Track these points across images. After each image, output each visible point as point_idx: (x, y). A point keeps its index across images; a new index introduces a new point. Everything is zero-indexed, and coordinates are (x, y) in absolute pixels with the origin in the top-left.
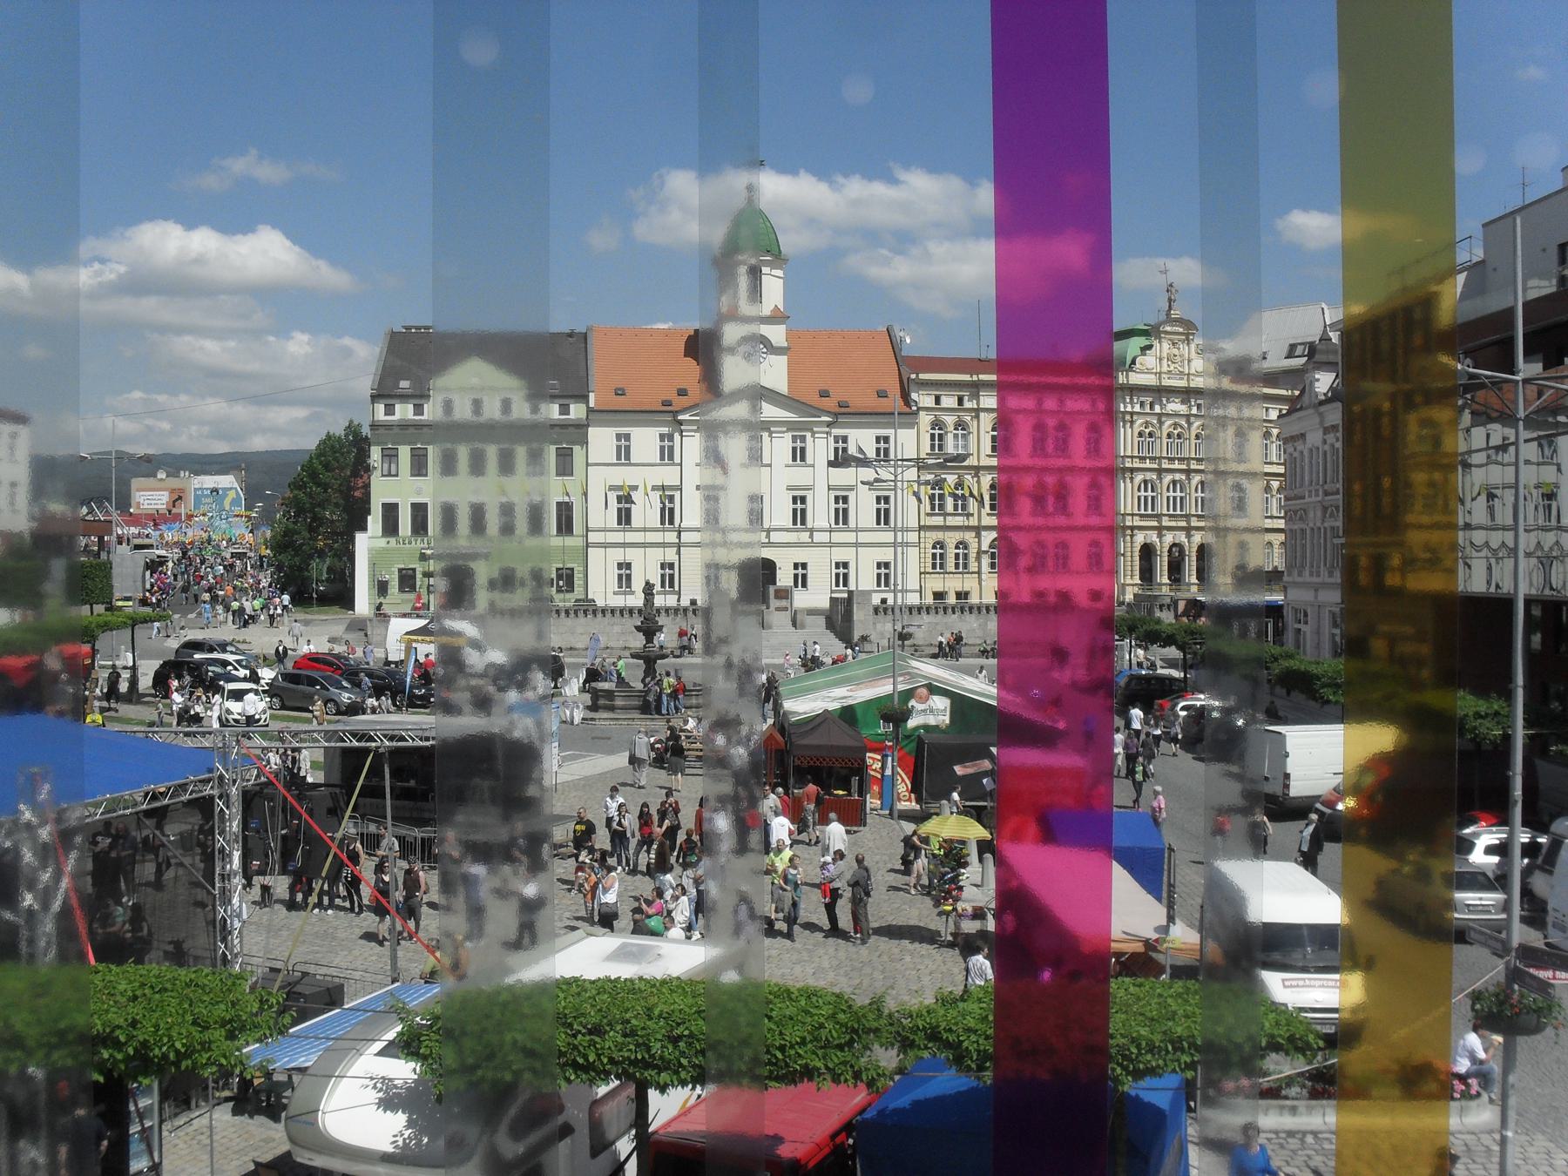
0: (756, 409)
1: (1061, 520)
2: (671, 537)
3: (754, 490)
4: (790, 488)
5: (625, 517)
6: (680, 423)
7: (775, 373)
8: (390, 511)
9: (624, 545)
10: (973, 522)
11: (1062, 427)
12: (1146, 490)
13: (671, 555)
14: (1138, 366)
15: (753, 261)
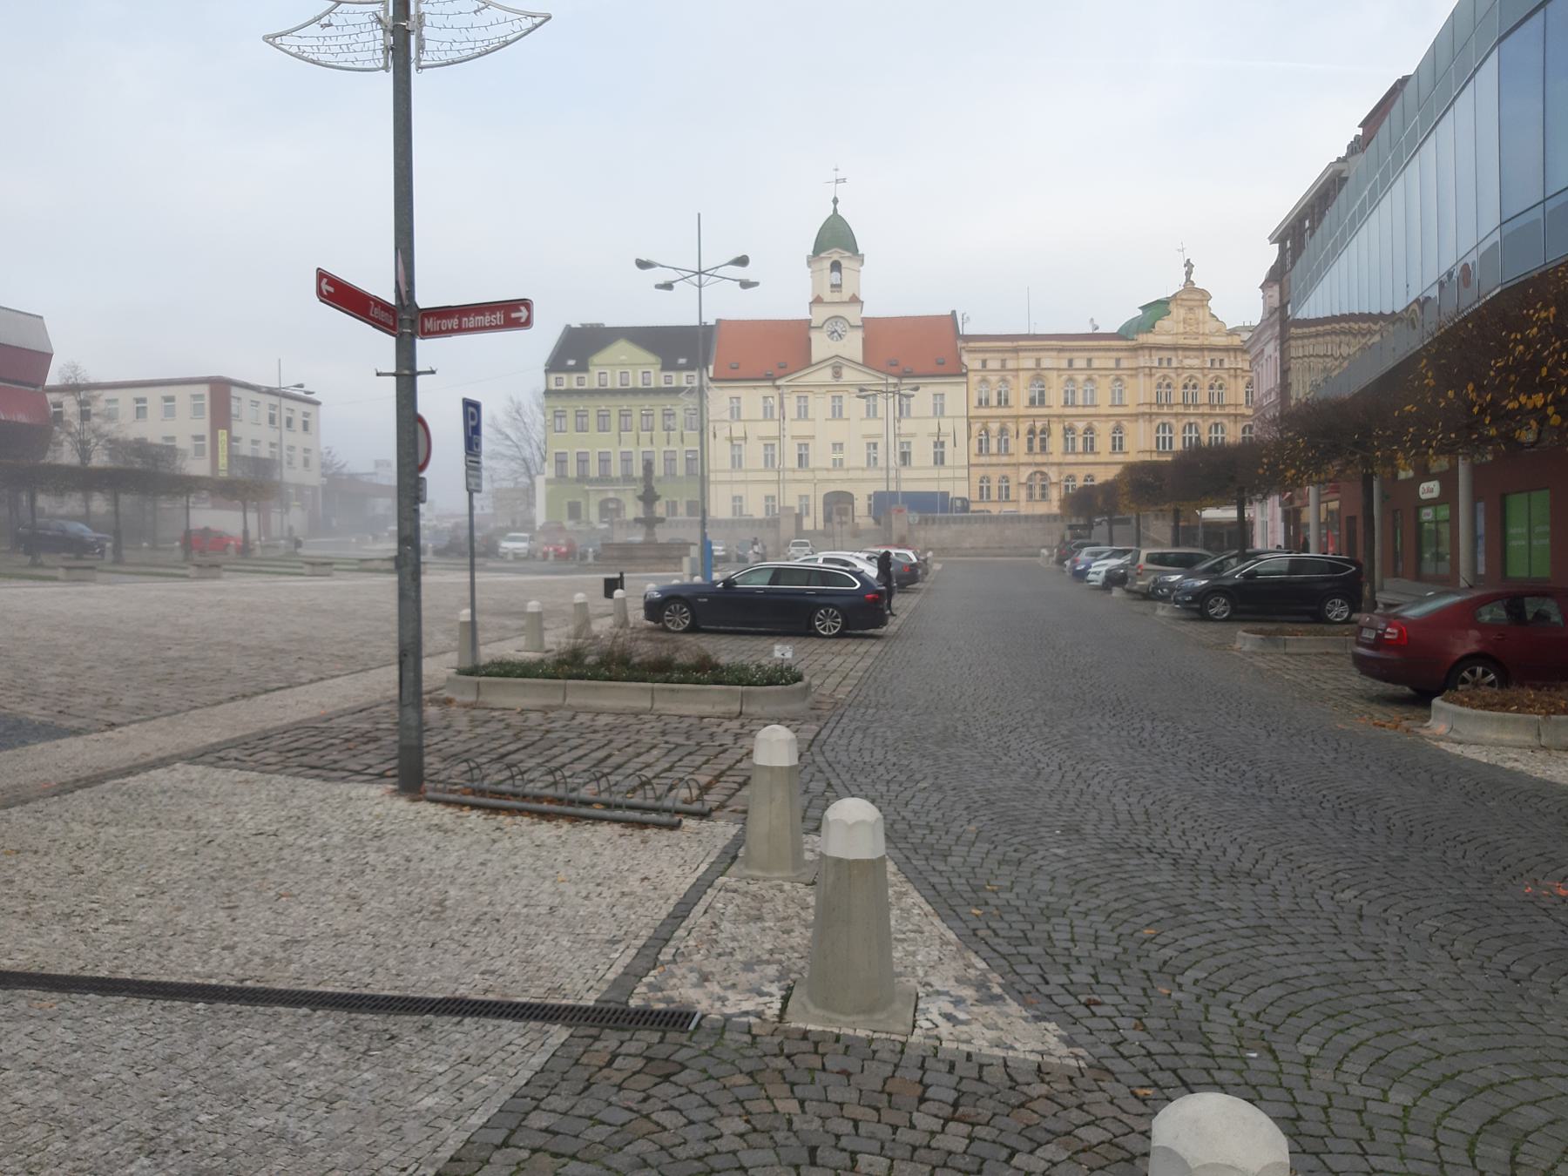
0: (837, 374)
1: (1090, 458)
2: (773, 476)
3: (838, 440)
4: (865, 436)
5: (737, 462)
6: (778, 387)
7: (853, 346)
8: (561, 460)
9: (730, 482)
10: (1013, 460)
11: (1090, 379)
12: (1164, 432)
13: (772, 490)
14: (1157, 329)
15: (836, 257)
